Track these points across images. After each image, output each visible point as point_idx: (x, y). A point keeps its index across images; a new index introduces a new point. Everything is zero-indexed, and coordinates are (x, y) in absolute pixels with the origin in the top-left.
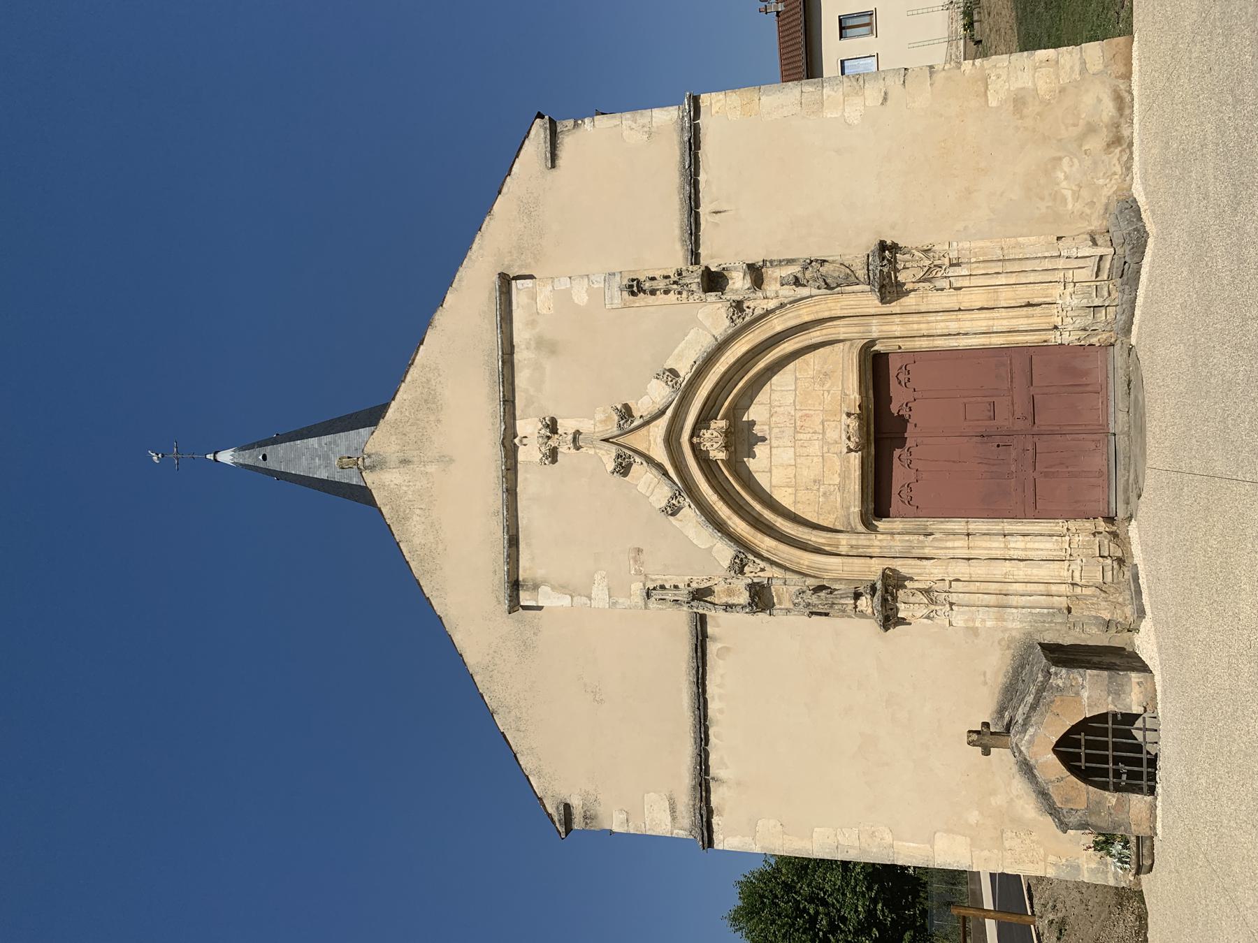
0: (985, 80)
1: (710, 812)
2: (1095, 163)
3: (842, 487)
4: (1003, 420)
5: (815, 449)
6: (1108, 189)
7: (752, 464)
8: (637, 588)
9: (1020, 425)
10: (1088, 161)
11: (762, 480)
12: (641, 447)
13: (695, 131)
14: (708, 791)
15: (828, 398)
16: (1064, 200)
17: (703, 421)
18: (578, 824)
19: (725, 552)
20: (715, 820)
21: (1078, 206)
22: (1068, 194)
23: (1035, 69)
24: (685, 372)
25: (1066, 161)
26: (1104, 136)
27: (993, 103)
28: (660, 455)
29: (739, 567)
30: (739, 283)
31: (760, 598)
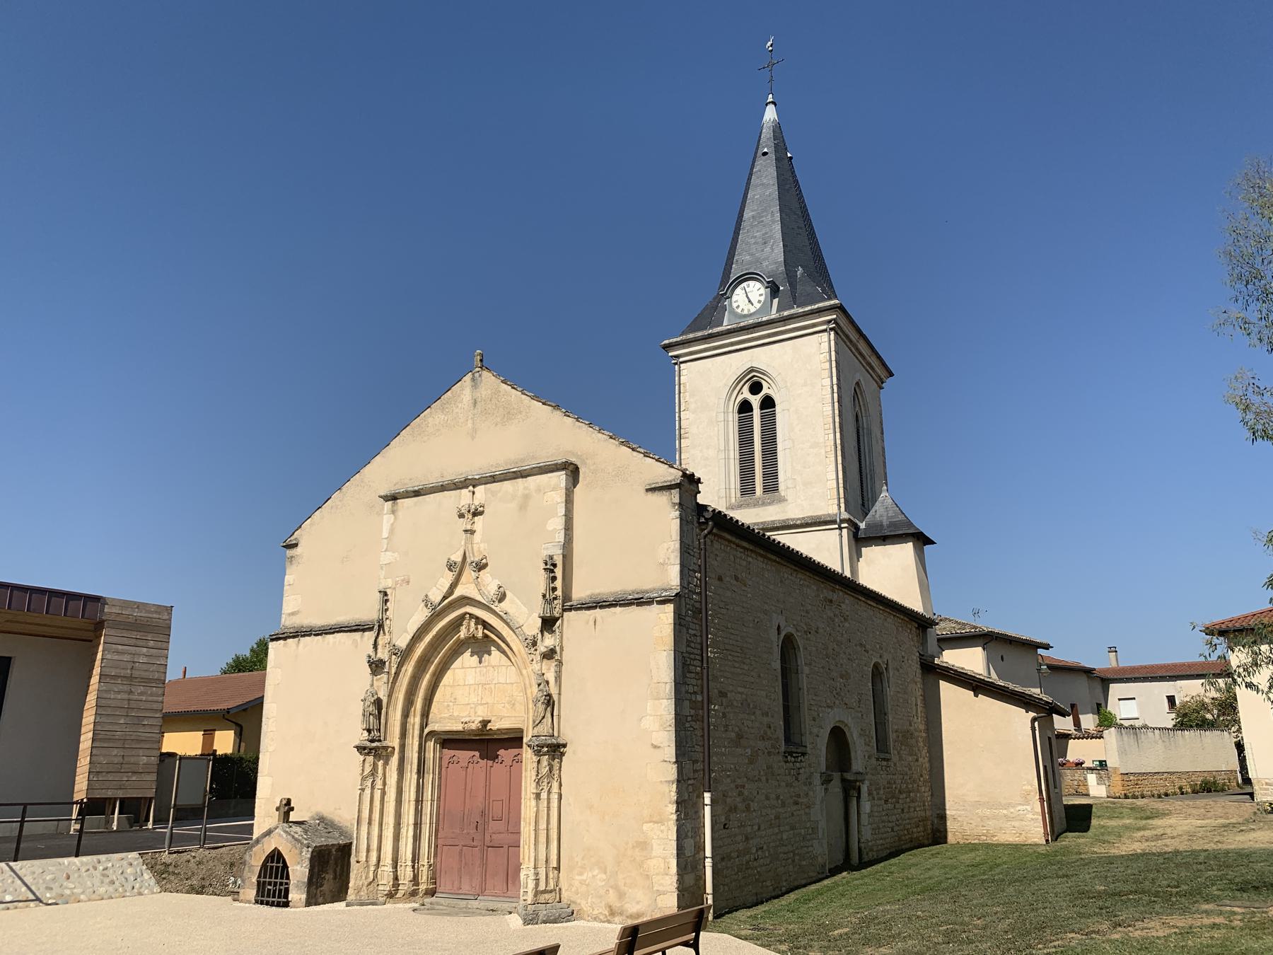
0: (661, 822)
1: (285, 639)
2: (601, 897)
3: (451, 717)
4: (493, 826)
5: (474, 699)
6: (584, 904)
7: (468, 653)
8: (389, 583)
9: (487, 838)
10: (602, 892)
11: (457, 663)
12: (463, 579)
13: (649, 602)
14: (294, 637)
15: (500, 706)
16: (581, 874)
17: (479, 621)
18: (289, 552)
19: (402, 642)
20: (281, 642)
21: (577, 883)
22: (584, 877)
23: (664, 858)
24: (498, 608)
25: (604, 876)
26: (616, 904)
27: (646, 827)
28: (458, 593)
29: (395, 651)
30: (549, 641)
31: (376, 666)
